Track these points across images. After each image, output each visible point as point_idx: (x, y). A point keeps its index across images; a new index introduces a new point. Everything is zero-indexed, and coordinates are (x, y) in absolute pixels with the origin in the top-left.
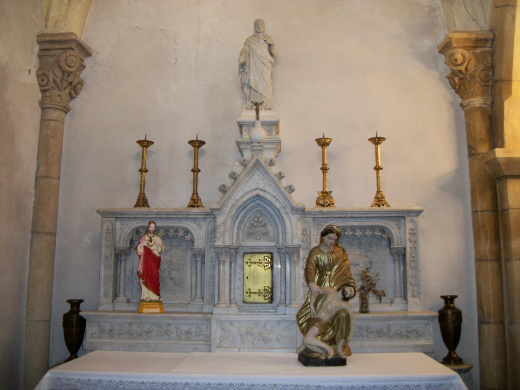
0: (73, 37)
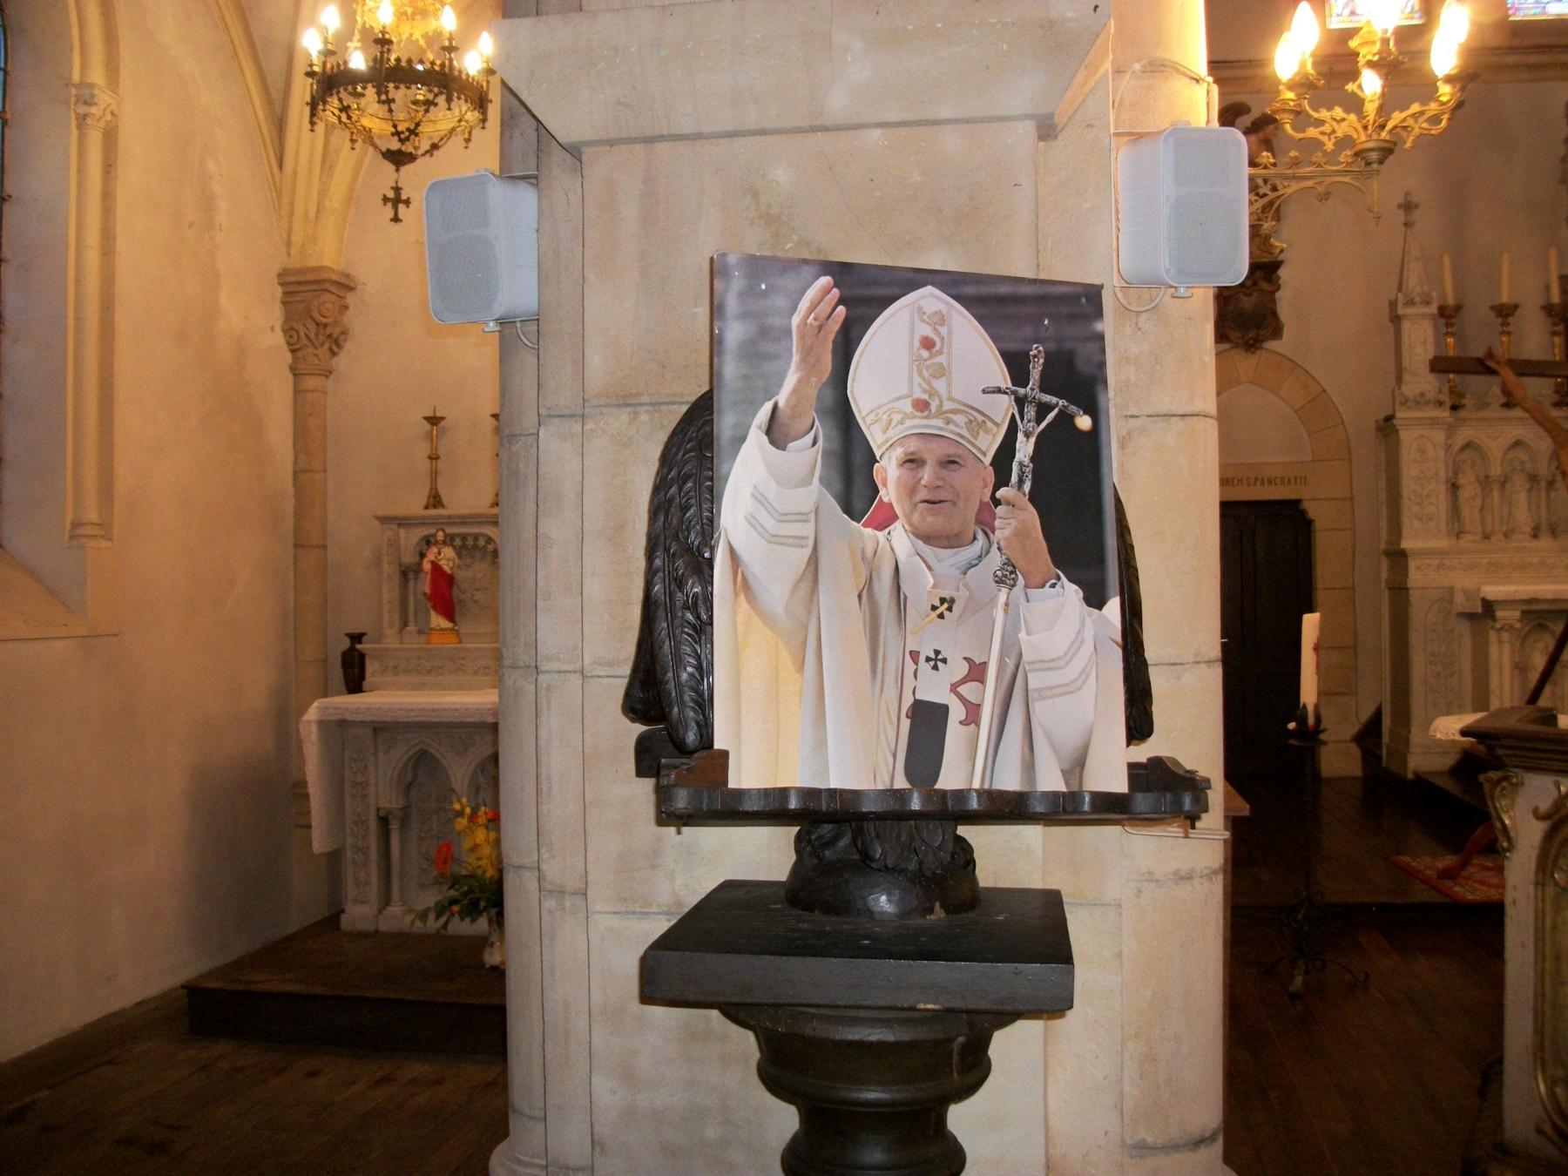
0: (325, 276)
